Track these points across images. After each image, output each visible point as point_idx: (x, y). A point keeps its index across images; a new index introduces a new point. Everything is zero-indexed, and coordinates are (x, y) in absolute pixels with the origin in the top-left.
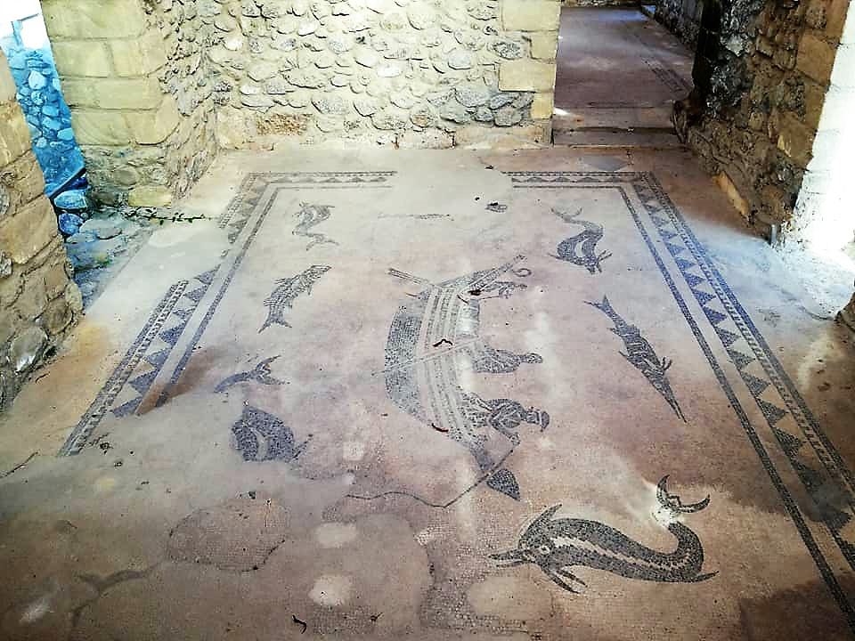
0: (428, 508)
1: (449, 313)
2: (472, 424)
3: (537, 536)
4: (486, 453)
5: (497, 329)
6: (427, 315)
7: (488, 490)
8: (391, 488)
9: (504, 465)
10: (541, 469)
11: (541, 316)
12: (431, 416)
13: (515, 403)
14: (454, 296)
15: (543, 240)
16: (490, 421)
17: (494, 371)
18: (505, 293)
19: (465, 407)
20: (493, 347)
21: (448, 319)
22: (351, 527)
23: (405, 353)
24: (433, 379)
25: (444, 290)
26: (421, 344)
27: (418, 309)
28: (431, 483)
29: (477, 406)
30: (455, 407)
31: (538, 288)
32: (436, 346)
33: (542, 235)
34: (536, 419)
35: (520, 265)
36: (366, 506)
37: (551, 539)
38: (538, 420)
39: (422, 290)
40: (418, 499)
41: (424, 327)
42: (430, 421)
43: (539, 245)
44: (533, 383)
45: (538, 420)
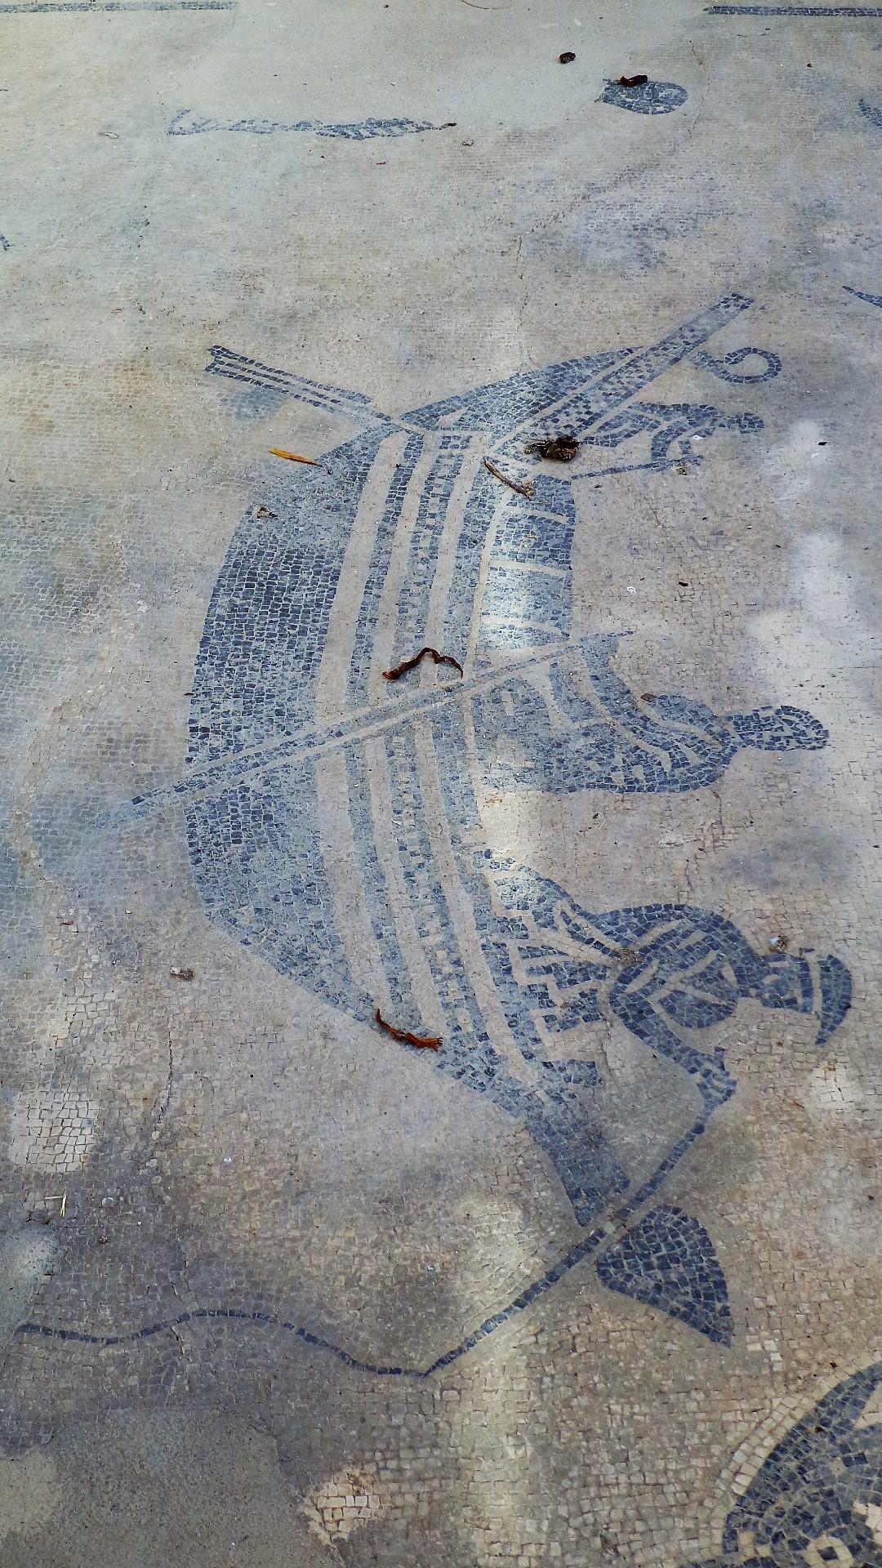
0: (351, 1381)
1: (449, 538)
2: (537, 1014)
3: (798, 1498)
4: (597, 1139)
5: (645, 606)
6: (361, 544)
7: (597, 1296)
8: (201, 1292)
9: (670, 1188)
10: (813, 1206)
11: (820, 547)
12: (373, 979)
13: (717, 921)
14: (472, 463)
15: (823, 233)
16: (613, 1000)
17: (631, 786)
18: (675, 450)
19: (512, 945)
20: (632, 681)
21: (446, 562)
22: (38, 1467)
23: (267, 709)
24: (381, 819)
25: (432, 439)
26: (334, 668)
27: (326, 519)
28: (369, 1268)
29: (559, 938)
30: (469, 938)
31: (807, 433)
32: (395, 676)
33: (824, 211)
34: (797, 992)
35: (735, 334)
36: (99, 1370)
37: (859, 1507)
38: (807, 993)
39: (338, 439)
40: (310, 1338)
41: (349, 594)
42: (368, 1000)
43: (809, 250)
44: (786, 833)
45: (807, 993)
